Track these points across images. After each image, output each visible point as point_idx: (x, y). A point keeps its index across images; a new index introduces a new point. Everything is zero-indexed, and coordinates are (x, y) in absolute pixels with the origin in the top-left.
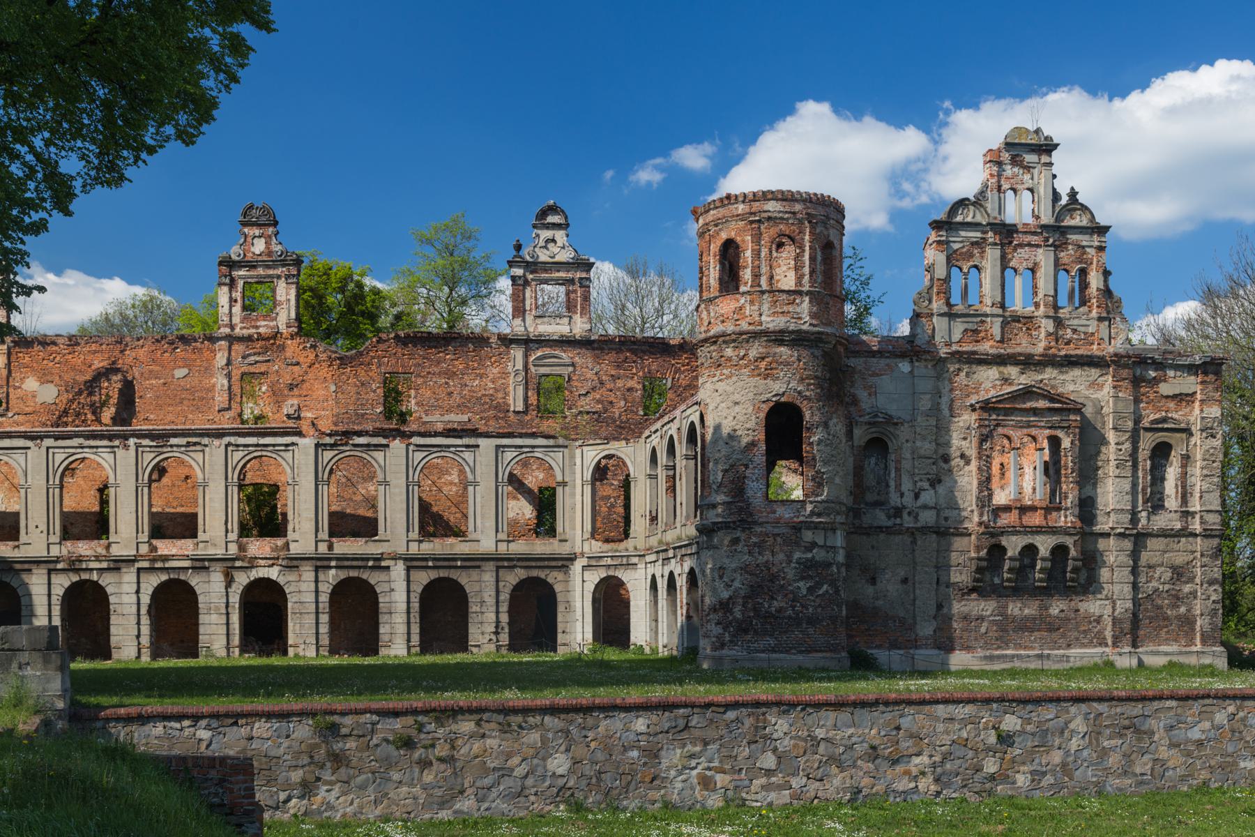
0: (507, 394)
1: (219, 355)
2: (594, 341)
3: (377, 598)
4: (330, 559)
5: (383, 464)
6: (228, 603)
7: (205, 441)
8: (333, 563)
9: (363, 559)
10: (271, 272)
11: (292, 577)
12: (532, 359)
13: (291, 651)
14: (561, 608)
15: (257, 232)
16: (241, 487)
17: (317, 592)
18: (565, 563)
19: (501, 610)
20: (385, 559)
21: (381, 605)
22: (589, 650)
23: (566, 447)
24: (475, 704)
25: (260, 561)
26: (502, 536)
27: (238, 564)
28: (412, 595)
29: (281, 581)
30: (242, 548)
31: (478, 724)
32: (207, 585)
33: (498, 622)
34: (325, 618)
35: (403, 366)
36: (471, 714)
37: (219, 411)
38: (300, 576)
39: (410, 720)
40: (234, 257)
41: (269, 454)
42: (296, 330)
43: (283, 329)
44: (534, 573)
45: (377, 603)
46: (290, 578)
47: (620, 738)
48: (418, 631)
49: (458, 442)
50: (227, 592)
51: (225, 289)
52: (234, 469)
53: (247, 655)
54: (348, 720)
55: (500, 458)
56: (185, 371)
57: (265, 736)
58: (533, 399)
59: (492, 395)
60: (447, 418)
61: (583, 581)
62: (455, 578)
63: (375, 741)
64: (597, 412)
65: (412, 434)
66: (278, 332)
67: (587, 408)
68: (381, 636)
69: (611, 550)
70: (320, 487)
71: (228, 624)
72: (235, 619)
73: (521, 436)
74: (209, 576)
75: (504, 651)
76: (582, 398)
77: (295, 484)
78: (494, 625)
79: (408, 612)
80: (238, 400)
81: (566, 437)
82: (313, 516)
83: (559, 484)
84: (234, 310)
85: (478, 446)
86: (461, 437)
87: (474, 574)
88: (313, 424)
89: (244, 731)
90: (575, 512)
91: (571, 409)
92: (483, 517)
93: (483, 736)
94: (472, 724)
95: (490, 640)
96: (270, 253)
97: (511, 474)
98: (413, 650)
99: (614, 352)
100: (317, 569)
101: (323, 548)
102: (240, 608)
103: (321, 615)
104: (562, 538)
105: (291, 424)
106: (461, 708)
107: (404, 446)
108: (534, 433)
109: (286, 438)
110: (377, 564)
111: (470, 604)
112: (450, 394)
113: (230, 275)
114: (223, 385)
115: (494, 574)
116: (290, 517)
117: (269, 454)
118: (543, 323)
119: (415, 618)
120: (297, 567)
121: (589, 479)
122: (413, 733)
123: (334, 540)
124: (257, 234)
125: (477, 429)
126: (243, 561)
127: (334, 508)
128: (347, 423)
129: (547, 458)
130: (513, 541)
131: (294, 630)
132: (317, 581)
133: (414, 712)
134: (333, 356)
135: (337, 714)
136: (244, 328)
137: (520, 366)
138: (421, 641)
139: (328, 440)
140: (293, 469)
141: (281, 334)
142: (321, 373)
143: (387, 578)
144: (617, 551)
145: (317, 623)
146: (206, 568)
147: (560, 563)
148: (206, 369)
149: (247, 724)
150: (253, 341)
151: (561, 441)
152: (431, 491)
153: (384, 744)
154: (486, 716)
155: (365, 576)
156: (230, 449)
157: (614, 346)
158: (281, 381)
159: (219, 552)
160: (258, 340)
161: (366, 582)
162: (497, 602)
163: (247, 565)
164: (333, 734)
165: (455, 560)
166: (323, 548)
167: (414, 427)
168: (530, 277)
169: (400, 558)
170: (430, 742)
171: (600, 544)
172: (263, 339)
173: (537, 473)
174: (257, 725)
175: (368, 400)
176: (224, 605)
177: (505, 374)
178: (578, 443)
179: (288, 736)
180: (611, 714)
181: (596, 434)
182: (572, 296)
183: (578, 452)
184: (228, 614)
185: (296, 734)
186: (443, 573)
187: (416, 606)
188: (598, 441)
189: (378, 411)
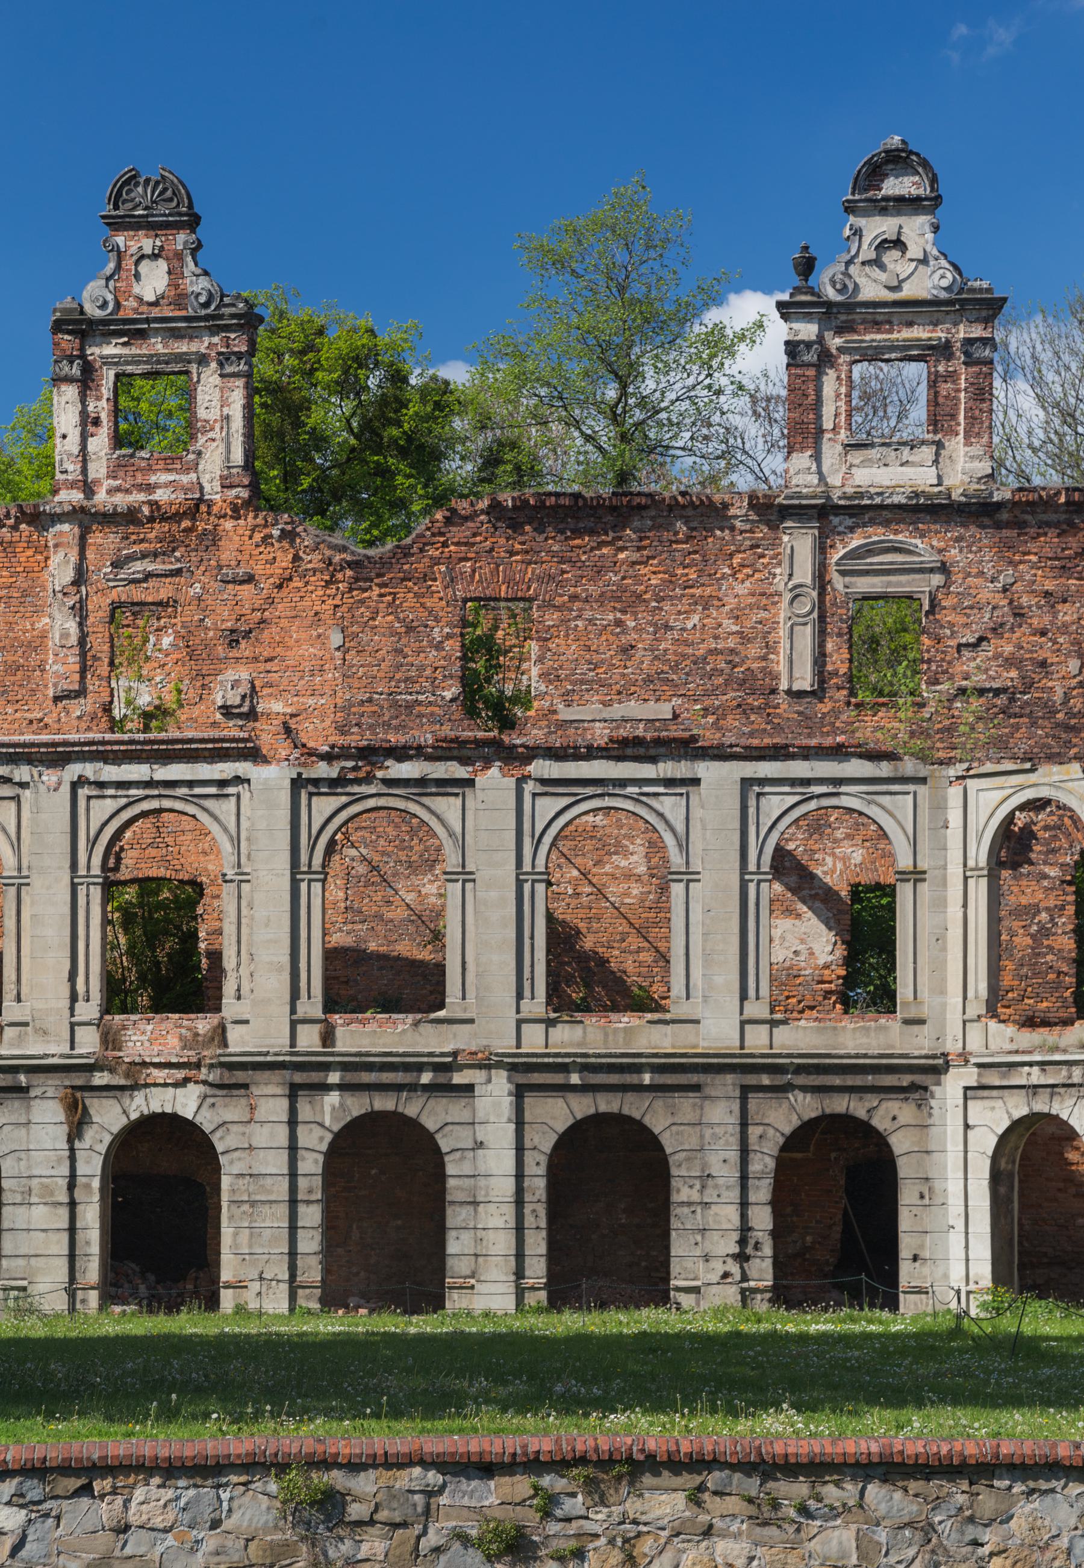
0: (770, 648)
1: (56, 559)
2: (999, 505)
3: (442, 1165)
4: (326, 1067)
5: (458, 829)
6: (73, 1176)
7: (22, 773)
8: (334, 1078)
9: (407, 1067)
10: (183, 347)
11: (233, 1110)
12: (835, 556)
13: (227, 1300)
14: (907, 1196)
15: (148, 245)
16: (109, 887)
17: (293, 1148)
18: (918, 1079)
19: (752, 1198)
20: (461, 1068)
21: (451, 1183)
22: (984, 1306)
23: (923, 780)
24: (685, 1447)
25: (155, 1072)
26: (757, 1009)
27: (100, 1079)
28: (529, 1158)
29: (206, 1121)
30: (110, 1039)
31: (695, 1498)
32: (23, 1131)
33: (745, 1229)
34: (311, 1216)
35: (508, 582)
36: (677, 1473)
37: (57, 699)
38: (252, 1108)
39: (521, 1485)
40: (92, 311)
41: (178, 805)
42: (245, 494)
43: (212, 490)
44: (839, 1104)
45: (440, 1176)
46: (228, 1117)
47: (1069, 1552)
48: (543, 1249)
49: (647, 771)
50: (72, 1150)
51: (70, 392)
52: (93, 843)
53: (118, 1309)
54: (366, 1484)
55: (752, 811)
57: (158, 1522)
58: (838, 660)
59: (732, 651)
60: (618, 711)
61: (967, 1126)
62: (637, 1115)
63: (432, 1538)
64: (1004, 690)
65: (533, 753)
66: (201, 499)
67: (979, 679)
68: (450, 1262)
69: (1041, 1048)
70: (304, 886)
71: (72, 1230)
72: (91, 1216)
73: (806, 753)
74: (28, 1108)
75: (761, 1305)
76: (967, 654)
77: (242, 879)
78: (736, 1236)
79: (519, 1201)
80: (104, 669)
81: (923, 757)
82: (286, 959)
83: (904, 876)
84: (93, 444)
85: (696, 782)
86: (653, 760)
87: (686, 1105)
88: (288, 730)
89: (106, 1511)
90: (944, 949)
91: (937, 682)
92: (708, 961)
93: (708, 1532)
94: (679, 1499)
95: (726, 1275)
96: (180, 299)
97: (781, 854)
98: (532, 1299)
99: (1052, 532)
100: (294, 1092)
101: (309, 1039)
102: (103, 1189)
103: (302, 1209)
104: (912, 1014)
105: (232, 729)
106: (651, 1457)
107: (511, 782)
108: (840, 746)
109: (221, 766)
110: (442, 1079)
111: (674, 1183)
112: (628, 650)
113: (83, 356)
114: (65, 635)
115: (736, 1106)
116: (229, 962)
117: (178, 805)
118: (866, 463)
119: (537, 1216)
120: (246, 1086)
121: (983, 861)
122: (530, 1517)
123: (337, 1018)
124: (148, 250)
125: (694, 739)
126: (112, 1071)
127: (338, 939)
128: (371, 727)
129: (873, 811)
130: (784, 1022)
131: (235, 1245)
132: (293, 1122)
133: (534, 1465)
134: (337, 559)
135: (340, 1466)
136: (118, 489)
137: (804, 574)
138: (551, 1274)
139: (323, 770)
140: (236, 842)
141: (210, 504)
142: (307, 603)
143: (466, 1116)
144: (1055, 1049)
145: (293, 1228)
146: (21, 1090)
147: (906, 1080)
148: (25, 594)
149: (114, 1492)
150: (138, 523)
151: (909, 766)
152: (577, 895)
153: (457, 1545)
154: (715, 1478)
155: (411, 1110)
156: (83, 792)
157: (1053, 517)
158: (208, 622)
159: (55, 1049)
160: (151, 519)
161: (414, 1124)
162: (744, 1178)
163: (123, 1082)
164: (328, 1519)
165: (637, 1069)
166: (309, 1039)
167: (535, 735)
168: (835, 342)
169: (499, 1065)
170: (573, 1544)
171: (1010, 1030)
172: (164, 519)
173: (846, 849)
174: (139, 1494)
175: (422, 668)
176: (63, 1183)
177: (766, 597)
178: (952, 772)
179: (215, 1524)
180: (1043, 1485)
181: (1001, 746)
182: (945, 388)
183: (954, 793)
184: (72, 1204)
185: (236, 1516)
186: (607, 1104)
187: (537, 1185)
188: (1009, 766)
189: (448, 695)
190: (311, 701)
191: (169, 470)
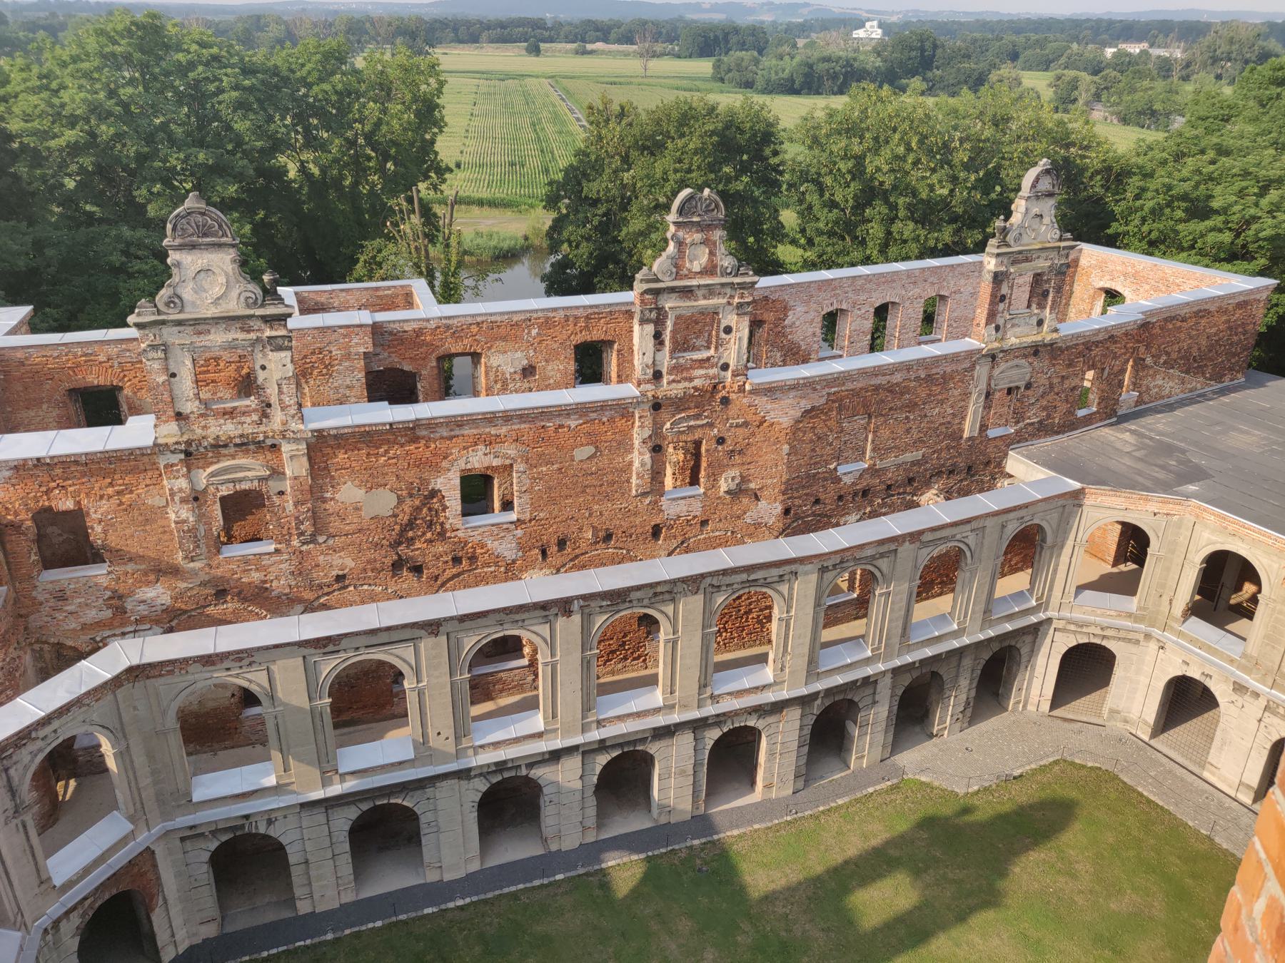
56: (590, 450)
128: (797, 489)
136: (674, 381)
142: (772, 433)
175: (822, 456)
190: (769, 481)
191: (702, 368)
